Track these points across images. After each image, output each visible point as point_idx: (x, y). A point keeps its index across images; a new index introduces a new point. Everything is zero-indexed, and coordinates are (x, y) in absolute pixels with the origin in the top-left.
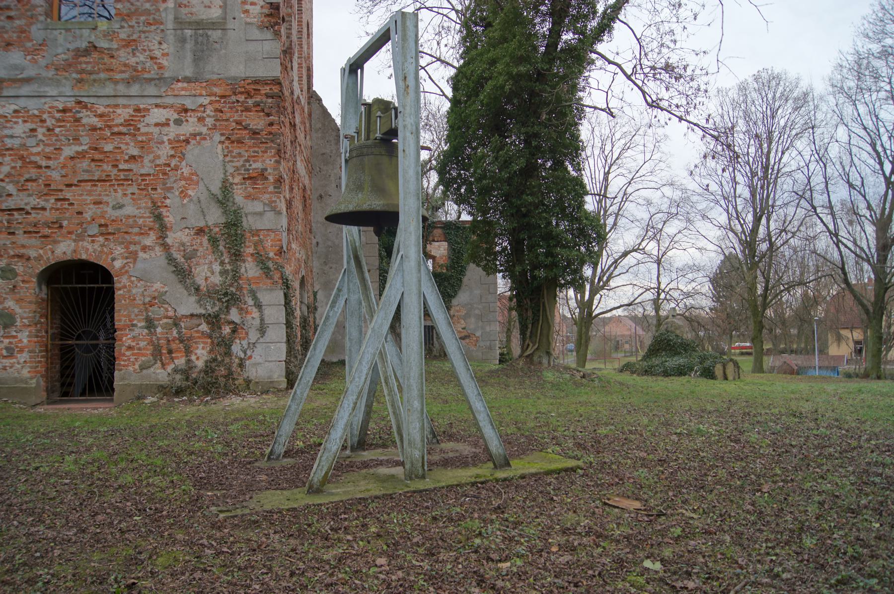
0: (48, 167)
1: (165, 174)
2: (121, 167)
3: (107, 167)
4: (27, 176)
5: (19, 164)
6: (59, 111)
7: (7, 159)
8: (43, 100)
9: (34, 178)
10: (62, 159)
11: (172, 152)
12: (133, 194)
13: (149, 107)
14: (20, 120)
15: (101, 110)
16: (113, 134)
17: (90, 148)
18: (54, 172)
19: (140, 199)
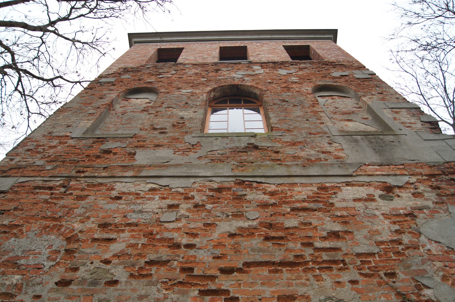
0: (189, 246)
1: (398, 253)
2: (318, 244)
3: (295, 246)
4: (153, 257)
5: (144, 240)
6: (211, 190)
7: (126, 234)
8: (192, 180)
9: (164, 258)
10: (215, 236)
11: (397, 227)
12: (353, 282)
13: (339, 185)
14: (157, 197)
15: (273, 188)
16: (293, 209)
17: (261, 224)
18: (201, 252)
19: (372, 291)
